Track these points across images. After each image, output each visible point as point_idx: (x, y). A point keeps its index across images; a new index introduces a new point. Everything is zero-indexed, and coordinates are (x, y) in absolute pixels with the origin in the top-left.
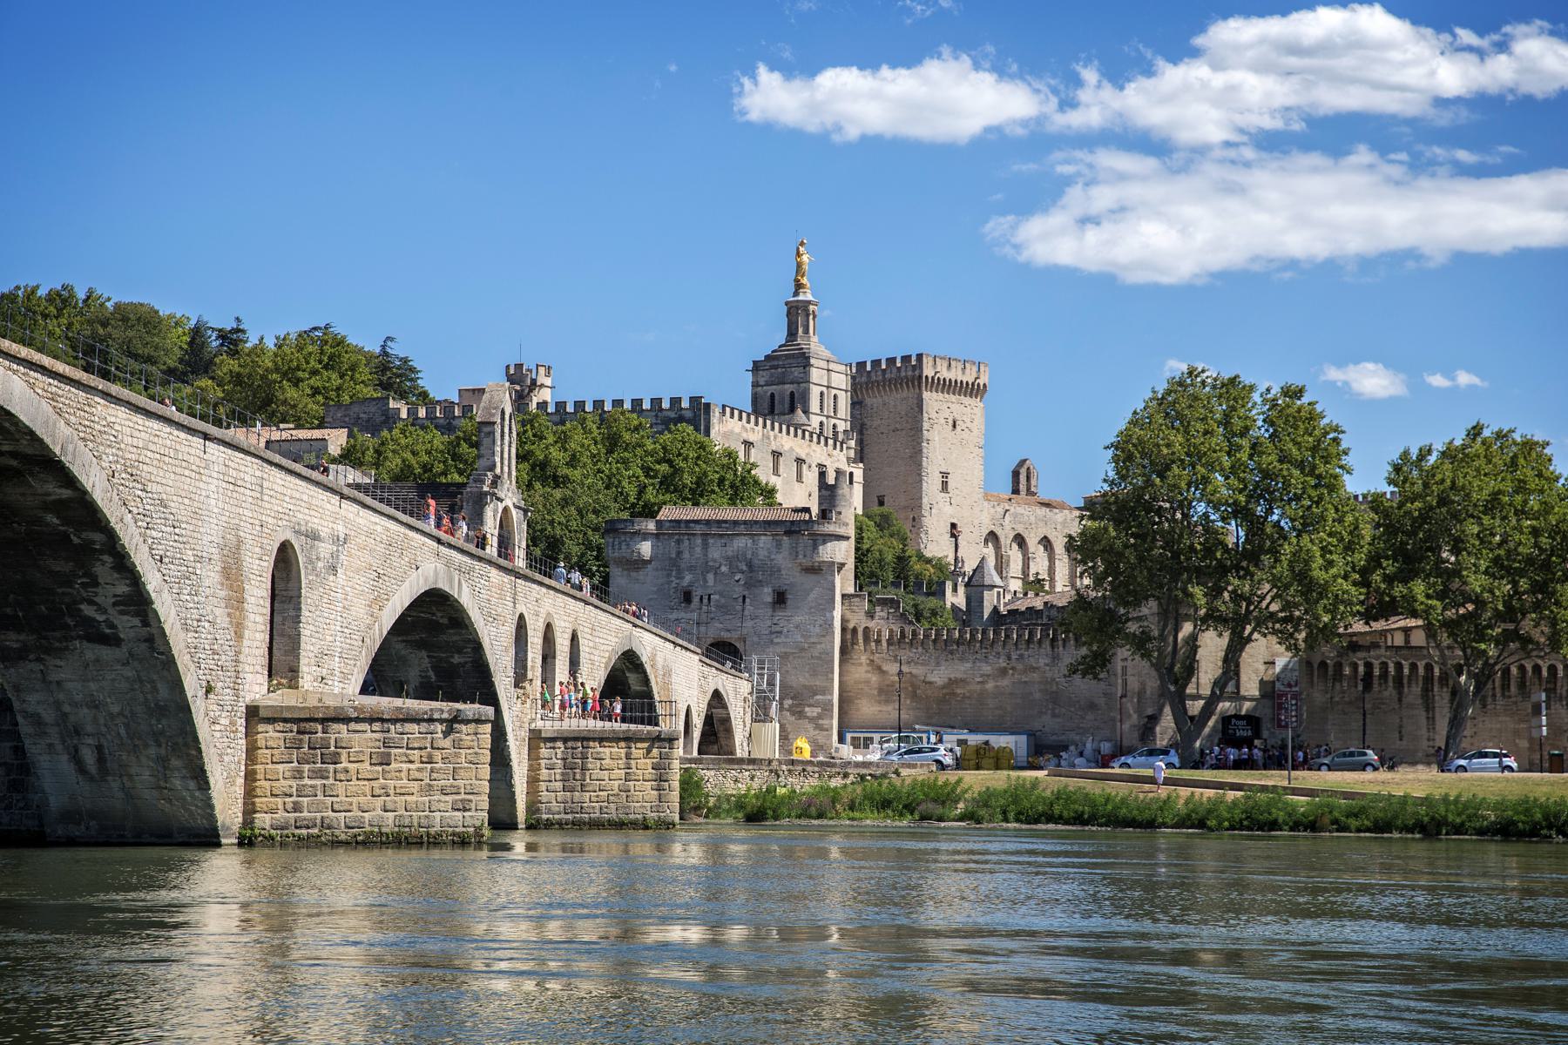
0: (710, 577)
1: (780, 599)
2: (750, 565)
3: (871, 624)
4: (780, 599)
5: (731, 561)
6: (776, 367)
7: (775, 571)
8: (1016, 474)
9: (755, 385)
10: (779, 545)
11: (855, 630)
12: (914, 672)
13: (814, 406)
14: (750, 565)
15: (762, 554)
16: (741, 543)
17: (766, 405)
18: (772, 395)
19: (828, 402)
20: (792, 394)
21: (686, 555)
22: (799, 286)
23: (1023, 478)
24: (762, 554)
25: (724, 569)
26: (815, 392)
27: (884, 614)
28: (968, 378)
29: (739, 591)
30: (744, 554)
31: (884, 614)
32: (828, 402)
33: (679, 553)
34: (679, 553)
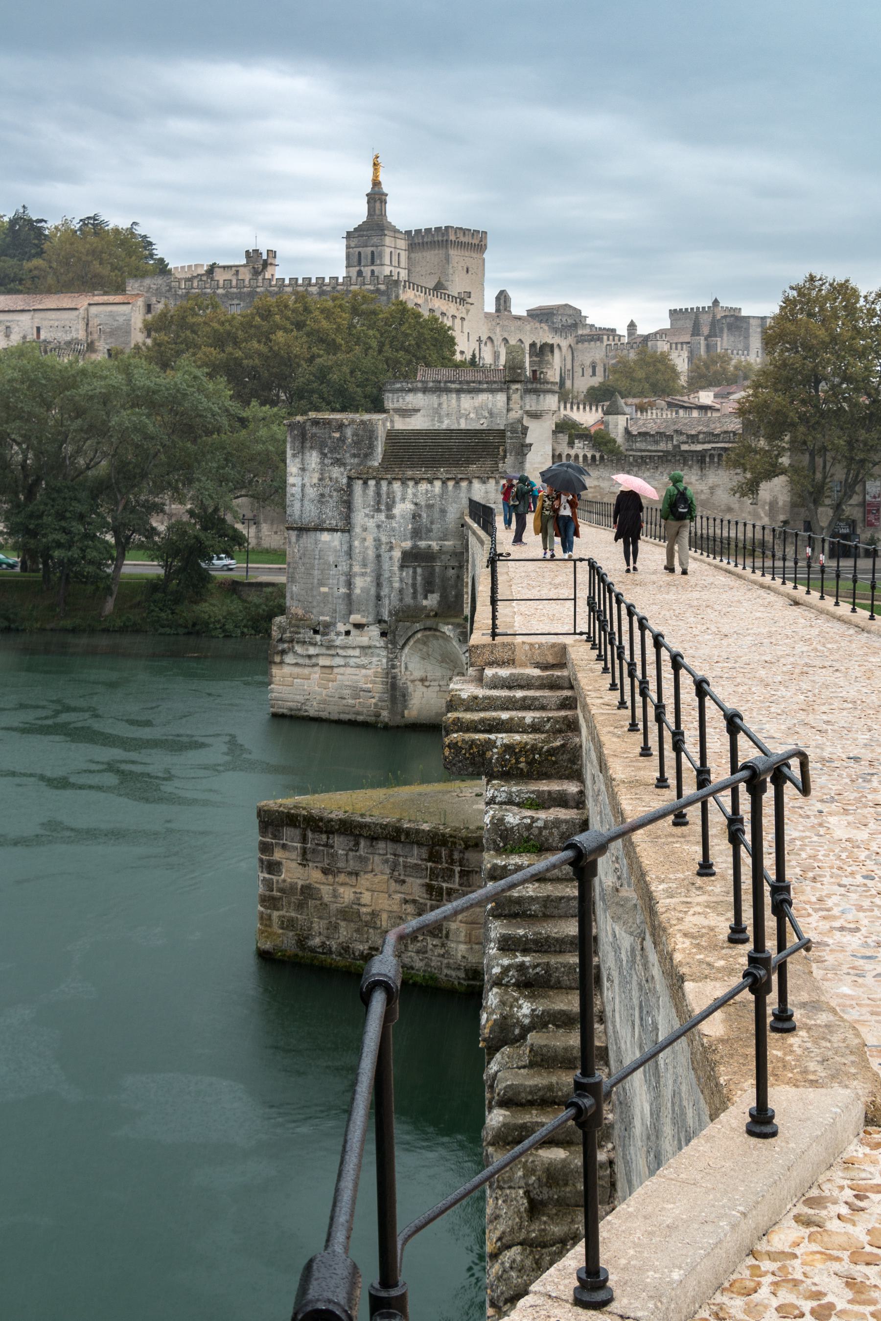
2: (491, 414)
3: (572, 453)
6: (362, 236)
8: (498, 299)
9: (348, 247)
11: (560, 456)
12: (602, 485)
13: (387, 261)
14: (491, 414)
16: (483, 397)
17: (356, 259)
18: (360, 253)
19: (395, 258)
20: (373, 253)
21: (445, 406)
22: (376, 183)
23: (502, 301)
25: (472, 415)
26: (388, 251)
27: (581, 445)
28: (476, 241)
30: (487, 405)
31: (581, 445)
32: (395, 258)
33: (440, 404)
34: (440, 404)
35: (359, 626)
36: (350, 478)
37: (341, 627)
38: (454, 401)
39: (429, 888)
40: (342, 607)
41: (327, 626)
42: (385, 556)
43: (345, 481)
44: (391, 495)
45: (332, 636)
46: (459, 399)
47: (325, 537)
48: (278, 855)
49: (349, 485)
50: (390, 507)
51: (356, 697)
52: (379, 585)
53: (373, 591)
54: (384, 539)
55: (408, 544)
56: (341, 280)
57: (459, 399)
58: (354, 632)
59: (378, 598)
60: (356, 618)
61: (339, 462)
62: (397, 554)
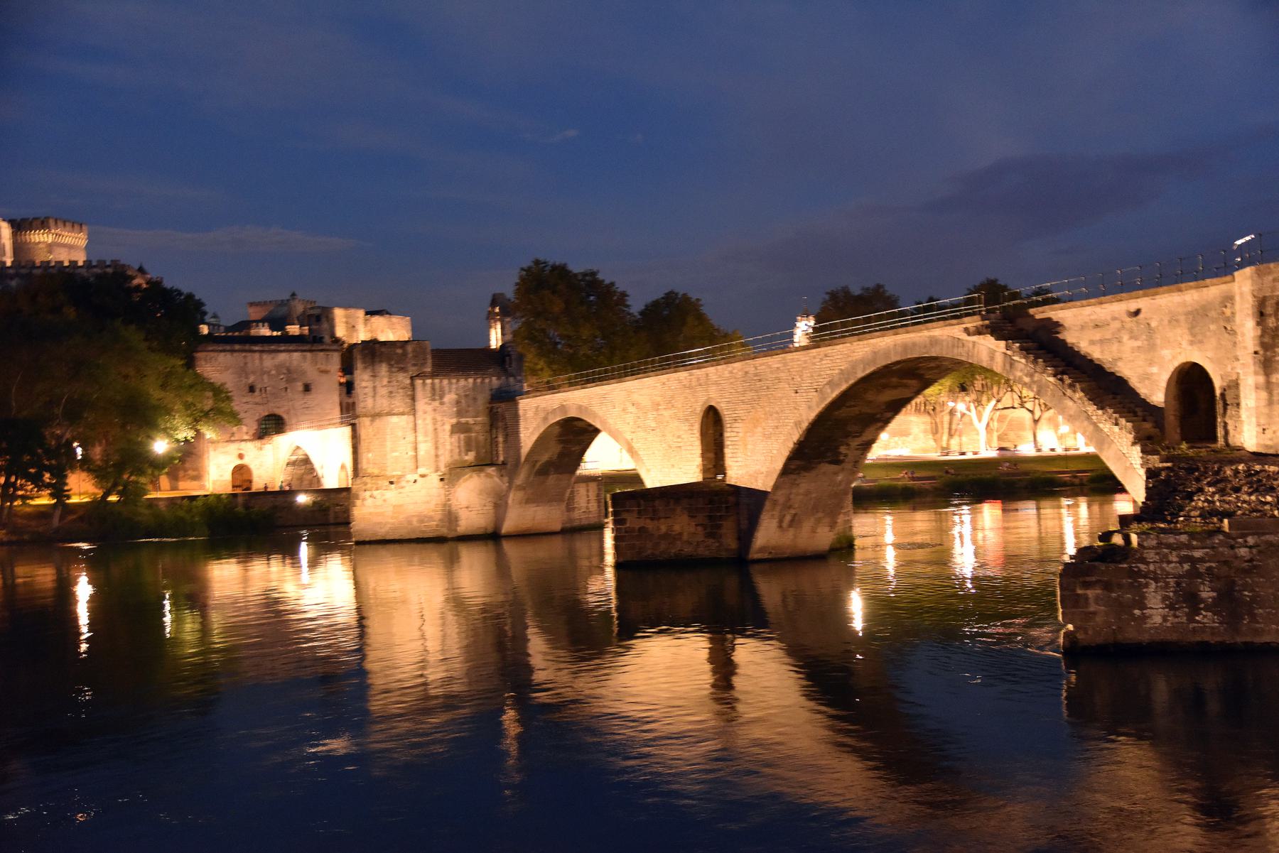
0: (265, 377)
1: (307, 388)
2: (289, 371)
4: (307, 388)
5: (278, 367)
7: (304, 373)
10: (305, 358)
15: (295, 363)
21: (249, 365)
24: (295, 363)
29: (283, 385)
35: (423, 476)
36: (412, 378)
37: (411, 477)
38: (257, 362)
39: (710, 517)
40: (411, 465)
41: (400, 477)
42: (440, 429)
43: (408, 381)
44: (442, 389)
45: (403, 484)
46: (261, 359)
47: (395, 419)
48: (624, 516)
49: (413, 385)
50: (441, 397)
51: (422, 521)
52: (437, 448)
53: (433, 452)
54: (439, 418)
55: (454, 421)
56: (80, 264)
57: (261, 359)
58: (420, 480)
59: (437, 456)
60: (422, 470)
61: (403, 370)
62: (448, 427)
